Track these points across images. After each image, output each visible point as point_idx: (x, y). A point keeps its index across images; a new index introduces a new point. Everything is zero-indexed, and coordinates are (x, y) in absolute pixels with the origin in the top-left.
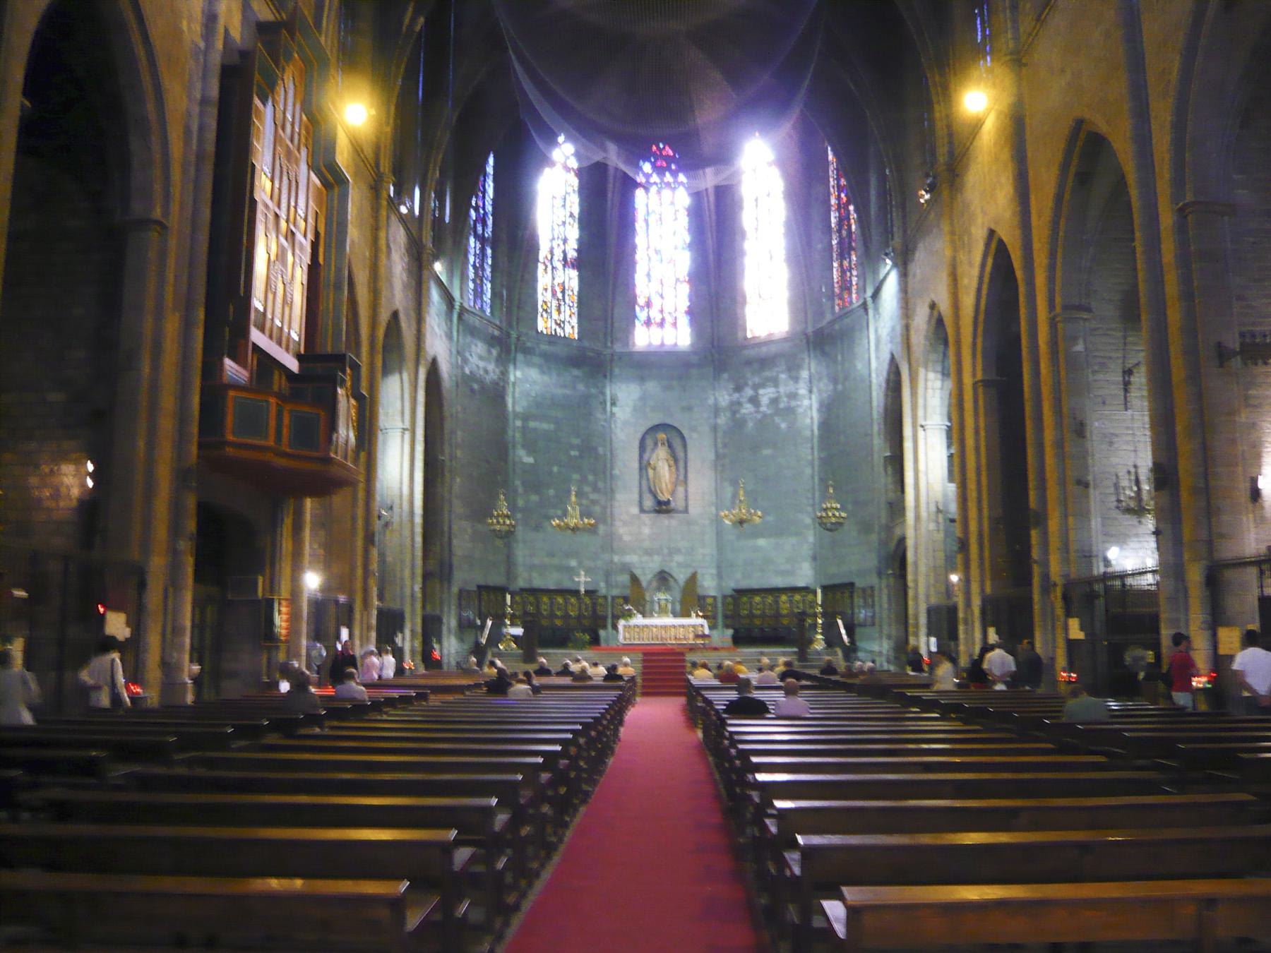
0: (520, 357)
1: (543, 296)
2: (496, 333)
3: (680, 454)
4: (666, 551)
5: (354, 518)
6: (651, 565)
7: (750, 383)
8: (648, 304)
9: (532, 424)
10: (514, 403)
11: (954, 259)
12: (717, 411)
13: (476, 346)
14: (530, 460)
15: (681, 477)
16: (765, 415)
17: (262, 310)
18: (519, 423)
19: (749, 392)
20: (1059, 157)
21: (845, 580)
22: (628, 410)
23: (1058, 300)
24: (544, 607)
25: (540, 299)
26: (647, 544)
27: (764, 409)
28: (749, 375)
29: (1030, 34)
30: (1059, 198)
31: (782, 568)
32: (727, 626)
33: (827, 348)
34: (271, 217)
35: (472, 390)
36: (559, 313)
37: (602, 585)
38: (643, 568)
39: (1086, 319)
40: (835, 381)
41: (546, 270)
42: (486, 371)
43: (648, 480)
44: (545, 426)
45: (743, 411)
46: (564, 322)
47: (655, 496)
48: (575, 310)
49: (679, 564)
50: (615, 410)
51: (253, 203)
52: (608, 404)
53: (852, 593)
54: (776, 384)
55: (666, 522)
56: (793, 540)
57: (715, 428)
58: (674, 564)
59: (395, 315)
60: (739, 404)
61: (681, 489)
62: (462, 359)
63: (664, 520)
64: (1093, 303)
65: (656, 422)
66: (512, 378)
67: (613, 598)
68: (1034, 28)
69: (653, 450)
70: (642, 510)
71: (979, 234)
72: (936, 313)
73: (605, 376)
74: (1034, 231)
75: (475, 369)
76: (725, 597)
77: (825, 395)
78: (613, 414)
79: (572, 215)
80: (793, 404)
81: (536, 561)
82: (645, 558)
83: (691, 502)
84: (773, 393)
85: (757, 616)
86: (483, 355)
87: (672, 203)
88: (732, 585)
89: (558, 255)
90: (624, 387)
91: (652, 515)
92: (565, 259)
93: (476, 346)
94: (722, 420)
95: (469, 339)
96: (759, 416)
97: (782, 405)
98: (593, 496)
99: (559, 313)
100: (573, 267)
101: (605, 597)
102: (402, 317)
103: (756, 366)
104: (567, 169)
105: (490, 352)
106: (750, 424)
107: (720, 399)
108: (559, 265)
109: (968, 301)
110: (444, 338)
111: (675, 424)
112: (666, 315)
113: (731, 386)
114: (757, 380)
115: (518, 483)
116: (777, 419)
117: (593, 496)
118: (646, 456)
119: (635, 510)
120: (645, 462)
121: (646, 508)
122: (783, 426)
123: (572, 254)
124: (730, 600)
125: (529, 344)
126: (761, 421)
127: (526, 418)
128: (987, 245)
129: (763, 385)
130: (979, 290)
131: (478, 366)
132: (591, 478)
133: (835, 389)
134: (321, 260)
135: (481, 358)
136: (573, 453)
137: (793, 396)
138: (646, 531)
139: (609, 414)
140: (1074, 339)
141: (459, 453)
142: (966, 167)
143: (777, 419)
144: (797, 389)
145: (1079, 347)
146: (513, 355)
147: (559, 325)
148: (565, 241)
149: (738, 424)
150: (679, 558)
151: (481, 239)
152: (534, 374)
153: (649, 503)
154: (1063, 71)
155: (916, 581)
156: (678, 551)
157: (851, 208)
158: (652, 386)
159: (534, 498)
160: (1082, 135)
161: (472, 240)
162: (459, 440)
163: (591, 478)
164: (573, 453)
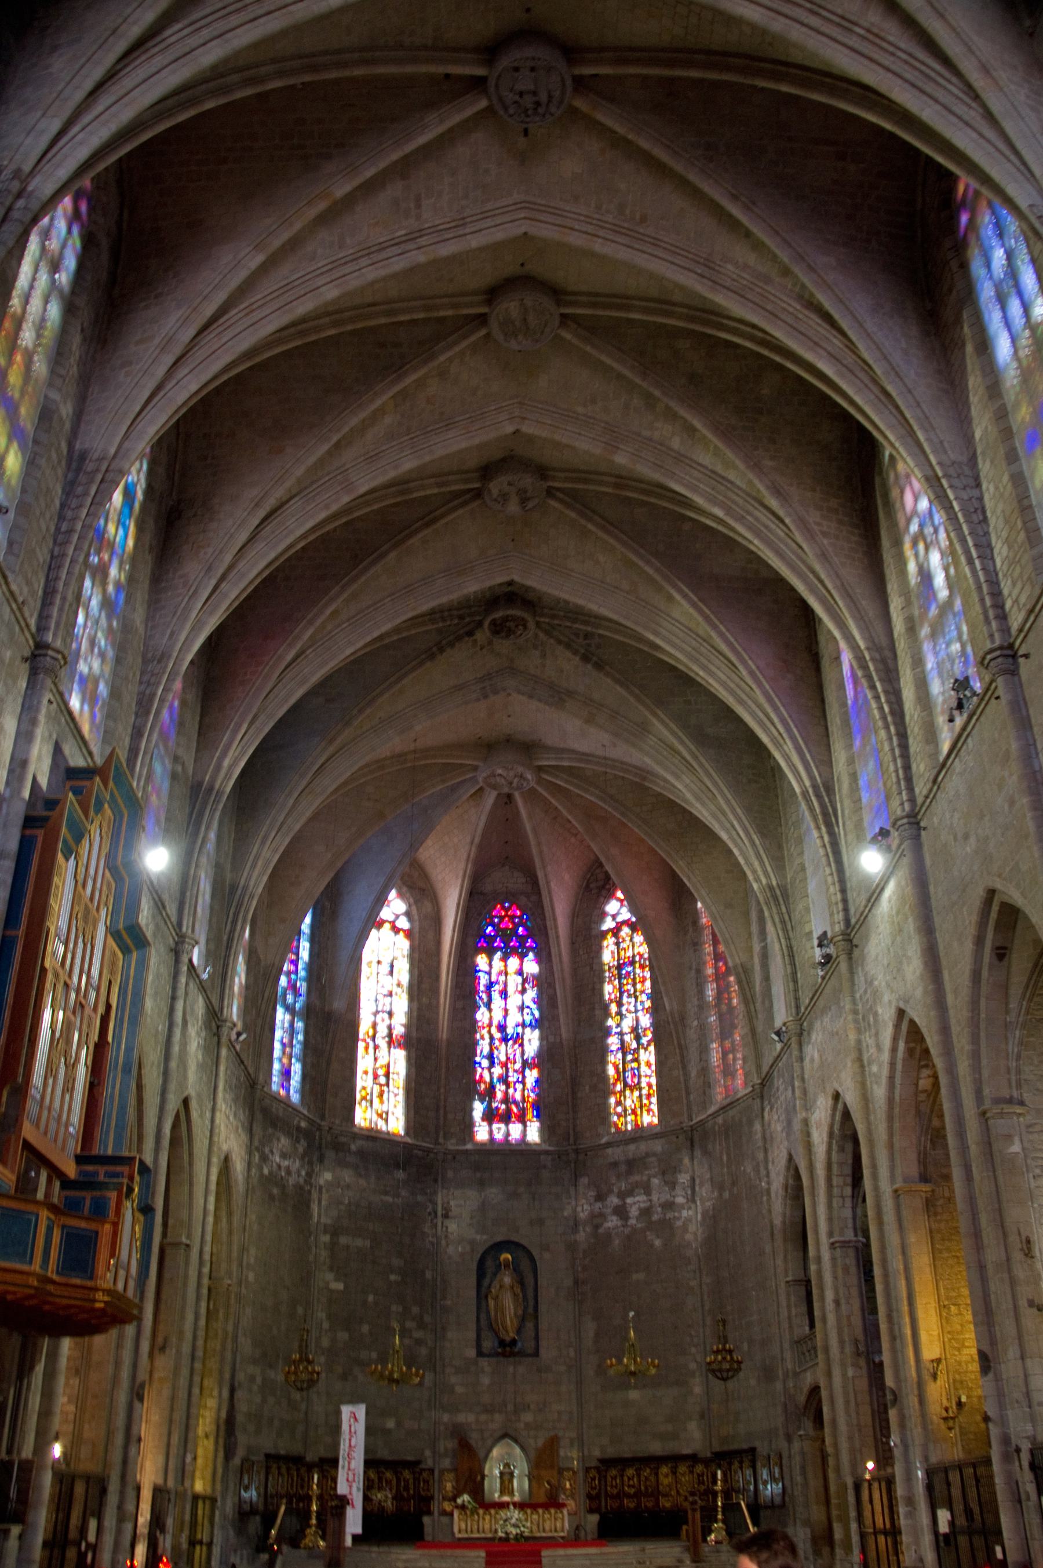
0: (330, 1154)
1: (363, 1082)
2: (303, 1124)
3: (529, 1280)
4: (510, 1407)
5: (118, 1364)
7: (616, 1190)
9: (343, 1240)
10: (319, 1216)
11: (859, 1042)
12: (575, 1224)
13: (278, 1140)
14: (340, 1286)
15: (531, 1310)
16: (634, 1230)
17: (38, 1097)
18: (326, 1238)
19: (614, 1200)
20: (971, 931)
21: (745, 1446)
23: (986, 1091)
25: (359, 1084)
27: (632, 1222)
28: (613, 1180)
29: (927, 797)
30: (976, 976)
32: (591, 1511)
33: (710, 1147)
34: (60, 987)
35: (272, 1197)
36: (382, 1102)
37: (428, 1453)
39: (1020, 1114)
40: (721, 1188)
41: (367, 1048)
42: (289, 1172)
43: (488, 1312)
44: (359, 1242)
45: (610, 1224)
46: (387, 1113)
47: (496, 1334)
49: (527, 1425)
50: (447, 1222)
51: (44, 970)
54: (647, 1191)
59: (186, 1102)
60: (602, 1216)
61: (530, 1325)
62: (260, 1157)
64: (1025, 1095)
65: (499, 1238)
67: (442, 1472)
68: (931, 790)
69: (495, 1274)
70: (480, 1354)
71: (886, 1014)
72: (840, 1106)
73: (436, 1181)
74: (952, 1012)
76: (587, 1470)
77: (708, 1204)
79: (399, 985)
80: (669, 1215)
82: (483, 1417)
83: (543, 1343)
84: (644, 1202)
85: (629, 1496)
87: (520, 972)
88: (597, 1453)
89: (382, 1030)
91: (493, 1360)
92: (390, 1035)
94: (581, 1236)
95: (270, 1130)
96: (627, 1231)
97: (655, 1217)
98: (418, 1334)
99: (382, 1102)
100: (400, 1046)
101: (432, 1471)
102: (194, 1105)
103: (623, 1168)
104: (396, 930)
107: (579, 1209)
108: (382, 1043)
109: (879, 1093)
111: (524, 1242)
113: (592, 1193)
115: (322, 1315)
116: (650, 1236)
117: (418, 1334)
118: (486, 1282)
119: (471, 1353)
120: (484, 1290)
121: (485, 1351)
122: (658, 1243)
123: (399, 1030)
124: (593, 1473)
127: (335, 1231)
128: (897, 1026)
129: (630, 1193)
130: (891, 1078)
131: (279, 1166)
132: (415, 1310)
133: (721, 1195)
134: (110, 1039)
135: (284, 1156)
137: (669, 1206)
140: (1009, 1138)
141: (251, 1277)
142: (866, 938)
143: (650, 1236)
145: (1016, 1148)
147: (380, 1116)
148: (390, 1014)
149: (601, 1241)
150: (528, 1417)
151: (290, 1009)
152: (347, 1176)
153: (488, 1344)
154: (966, 837)
155: (836, 1445)
156: (526, 1407)
157: (732, 979)
158: (494, 1194)
159: (343, 1336)
160: (995, 908)
161: (280, 1012)
163: (415, 1310)
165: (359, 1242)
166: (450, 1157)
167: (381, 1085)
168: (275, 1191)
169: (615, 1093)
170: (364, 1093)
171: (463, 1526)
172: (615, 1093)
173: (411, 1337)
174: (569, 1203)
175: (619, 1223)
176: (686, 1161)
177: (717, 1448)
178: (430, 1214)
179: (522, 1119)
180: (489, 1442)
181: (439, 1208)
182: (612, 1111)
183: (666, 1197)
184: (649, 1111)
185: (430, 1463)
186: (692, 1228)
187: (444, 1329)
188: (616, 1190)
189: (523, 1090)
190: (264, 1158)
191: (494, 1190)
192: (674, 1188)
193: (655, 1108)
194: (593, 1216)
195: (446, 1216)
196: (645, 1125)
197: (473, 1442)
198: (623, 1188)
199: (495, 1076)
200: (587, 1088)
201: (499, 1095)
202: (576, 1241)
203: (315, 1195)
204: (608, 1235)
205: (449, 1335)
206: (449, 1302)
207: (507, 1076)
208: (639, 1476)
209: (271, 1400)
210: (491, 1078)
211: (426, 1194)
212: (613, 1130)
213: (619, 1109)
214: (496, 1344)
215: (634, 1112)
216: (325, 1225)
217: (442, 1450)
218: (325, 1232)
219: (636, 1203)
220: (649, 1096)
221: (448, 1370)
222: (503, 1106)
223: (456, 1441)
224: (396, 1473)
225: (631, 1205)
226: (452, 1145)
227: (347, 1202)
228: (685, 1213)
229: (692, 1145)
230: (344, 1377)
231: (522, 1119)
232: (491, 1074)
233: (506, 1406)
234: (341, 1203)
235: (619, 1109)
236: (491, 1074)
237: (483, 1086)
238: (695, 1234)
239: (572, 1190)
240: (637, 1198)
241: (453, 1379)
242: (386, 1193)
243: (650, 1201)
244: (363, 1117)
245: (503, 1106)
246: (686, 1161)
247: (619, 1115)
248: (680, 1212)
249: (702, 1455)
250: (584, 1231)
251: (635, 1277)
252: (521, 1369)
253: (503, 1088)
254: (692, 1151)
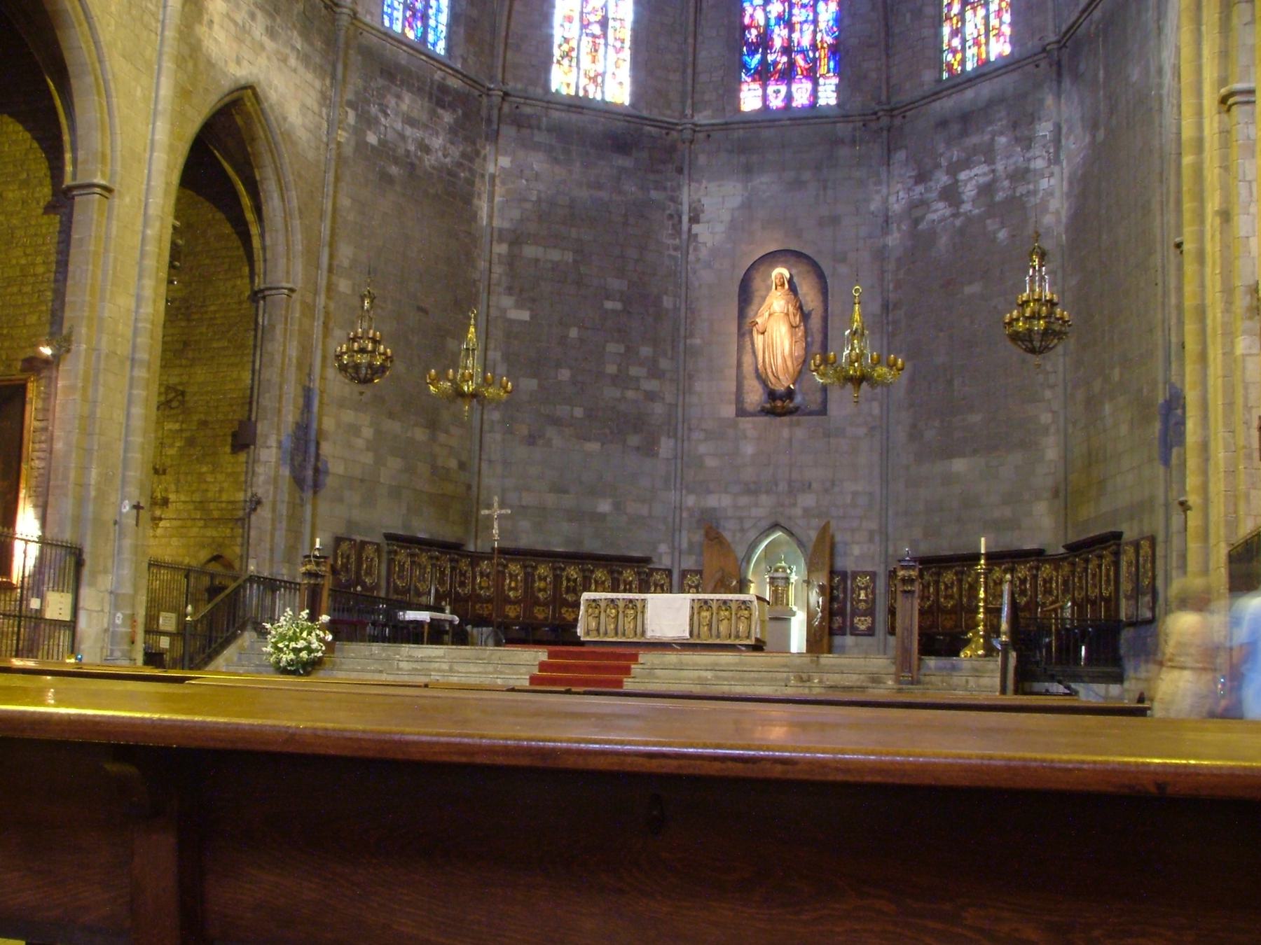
0: (508, 131)
2: (454, 83)
4: (783, 486)
6: (755, 512)
7: (944, 163)
8: (765, 41)
9: (530, 251)
10: (491, 217)
13: (399, 97)
14: (525, 315)
16: (969, 219)
18: (501, 249)
19: (943, 179)
22: (720, 228)
24: (539, 584)
25: (558, 34)
26: (748, 474)
27: (966, 207)
28: (941, 148)
31: (997, 514)
33: (1082, 67)
35: (386, 179)
37: (663, 548)
38: (741, 519)
42: (426, 149)
44: (555, 255)
45: (935, 216)
46: (603, 75)
48: (627, 54)
49: (806, 511)
50: (696, 228)
52: (685, 219)
53: (1117, 554)
54: (989, 154)
55: (786, 433)
56: (1016, 458)
57: (880, 255)
58: (798, 511)
60: (923, 203)
63: (782, 429)
65: (773, 248)
66: (491, 168)
70: (741, 412)
75: (391, 136)
76: (892, 574)
78: (692, 237)
80: (1021, 190)
81: (528, 499)
82: (744, 500)
84: (985, 174)
86: (415, 114)
90: (713, 186)
93: (399, 97)
94: (894, 239)
95: (381, 82)
96: (958, 222)
97: (1000, 196)
98: (652, 385)
103: (955, 128)
105: (433, 113)
106: (943, 241)
107: (892, 199)
110: (293, 61)
112: (799, 60)
114: (956, 154)
116: (991, 225)
117: (652, 385)
119: (729, 411)
122: (1002, 235)
125: (528, 110)
126: (962, 231)
127: (516, 239)
129: (966, 164)
131: (402, 137)
132: (646, 351)
133: (1094, 136)
135: (410, 121)
136: (609, 305)
138: (749, 449)
139: (685, 236)
143: (991, 225)
144: (1029, 160)
146: (495, 127)
147: (593, 79)
149: (921, 240)
150: (807, 500)
152: (537, 162)
159: (530, 384)
162: (346, 263)
164: (609, 305)
165: (555, 255)
166: (701, 136)
167: (594, 36)
168: (394, 170)
169: (949, 18)
170: (565, 47)
171: (593, 625)
172: (949, 18)
173: (638, 389)
174: (878, 192)
175: (948, 212)
176: (1049, 101)
177: (1073, 538)
178: (671, 217)
179: (812, 75)
180: (752, 535)
181: (685, 208)
182: (945, 47)
183: (1018, 159)
184: (998, 35)
185: (666, 562)
186: (1054, 204)
187: (691, 377)
188: (944, 163)
189: (815, 33)
190: (367, 121)
191: (765, 179)
192: (1029, 148)
193: (1007, 30)
194: (913, 205)
195: (694, 219)
196: (992, 58)
197: (727, 535)
198: (955, 159)
199: (773, 16)
200: (908, 16)
201: (778, 43)
202: (885, 246)
203: (482, 187)
204: (932, 235)
205: (698, 386)
206: (698, 341)
207: (791, 15)
208: (960, 581)
209: (394, 463)
210: (767, 19)
211: (665, 189)
212: (945, 75)
213: (956, 42)
214: (764, 397)
215: (977, 43)
216: (501, 230)
217: (685, 545)
218: (501, 240)
219: (972, 179)
220: (999, 13)
221: (696, 435)
222: (785, 59)
223: (702, 532)
224: (611, 572)
225: (966, 182)
226: (703, 118)
227: (534, 198)
228: (1044, 184)
229: (1059, 75)
230: (531, 440)
231: (812, 75)
232: (766, 13)
233: (776, 485)
234: (526, 200)
235: (956, 42)
236: (766, 13)
237: (754, 32)
238: (1058, 213)
239: (884, 176)
240: (976, 170)
241: (702, 449)
242: (599, 186)
243: (993, 171)
244: (562, 80)
245: (785, 59)
246: (1049, 101)
247: (954, 52)
248: (1036, 182)
249: (1050, 552)
250: (899, 229)
251: (969, 290)
252: (800, 433)
253: (785, 32)
254: (1059, 82)
